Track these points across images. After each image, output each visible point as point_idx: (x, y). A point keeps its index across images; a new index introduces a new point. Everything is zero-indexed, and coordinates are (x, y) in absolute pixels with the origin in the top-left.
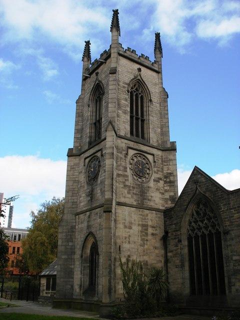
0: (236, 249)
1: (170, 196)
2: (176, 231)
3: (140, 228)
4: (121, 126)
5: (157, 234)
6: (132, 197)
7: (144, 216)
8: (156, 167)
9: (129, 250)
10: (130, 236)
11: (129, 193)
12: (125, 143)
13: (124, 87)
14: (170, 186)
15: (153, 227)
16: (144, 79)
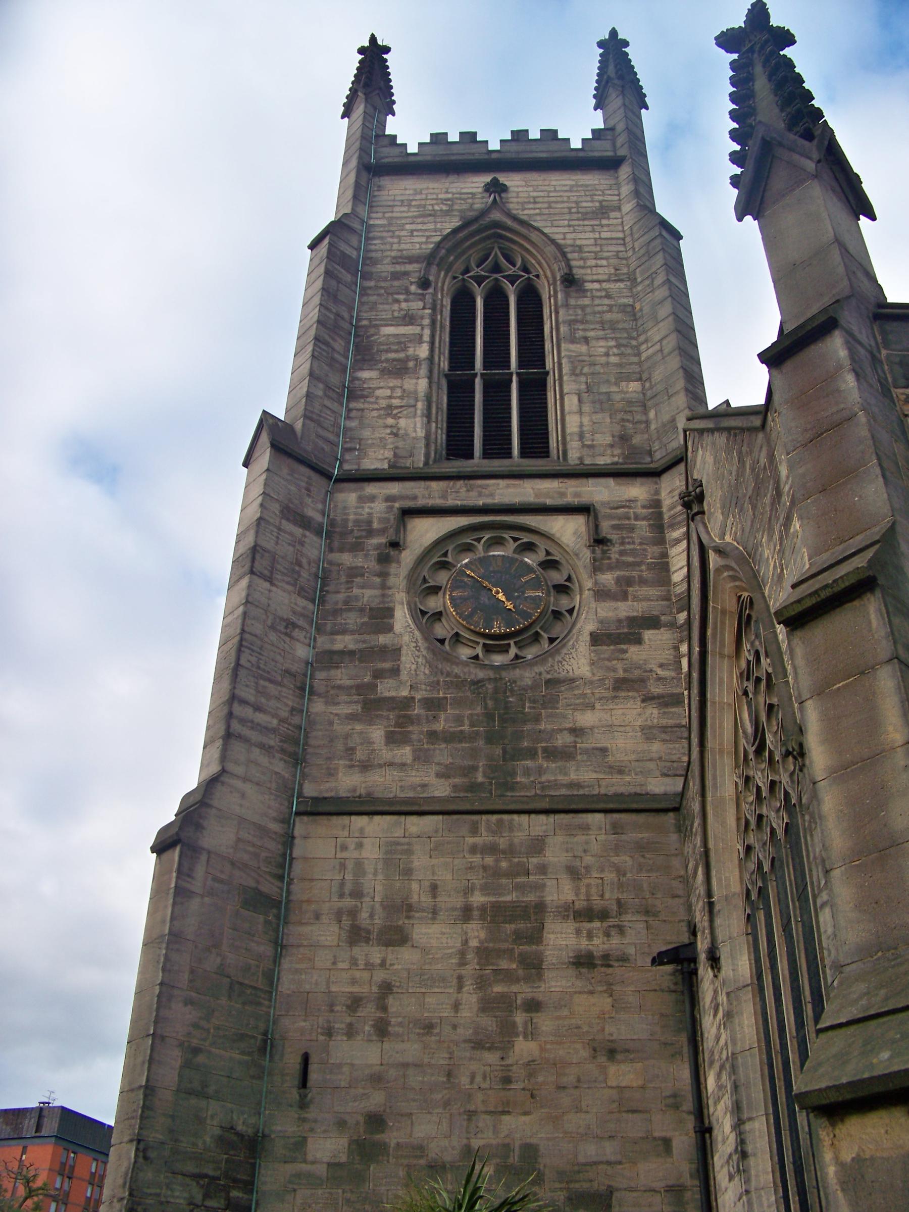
3: (476, 932)
4: (366, 433)
5: (624, 959)
6: (422, 757)
7: (511, 851)
8: (610, 568)
9: (377, 1079)
10: (387, 988)
11: (392, 739)
12: (389, 499)
13: (396, 276)
15: (587, 914)
16: (523, 215)
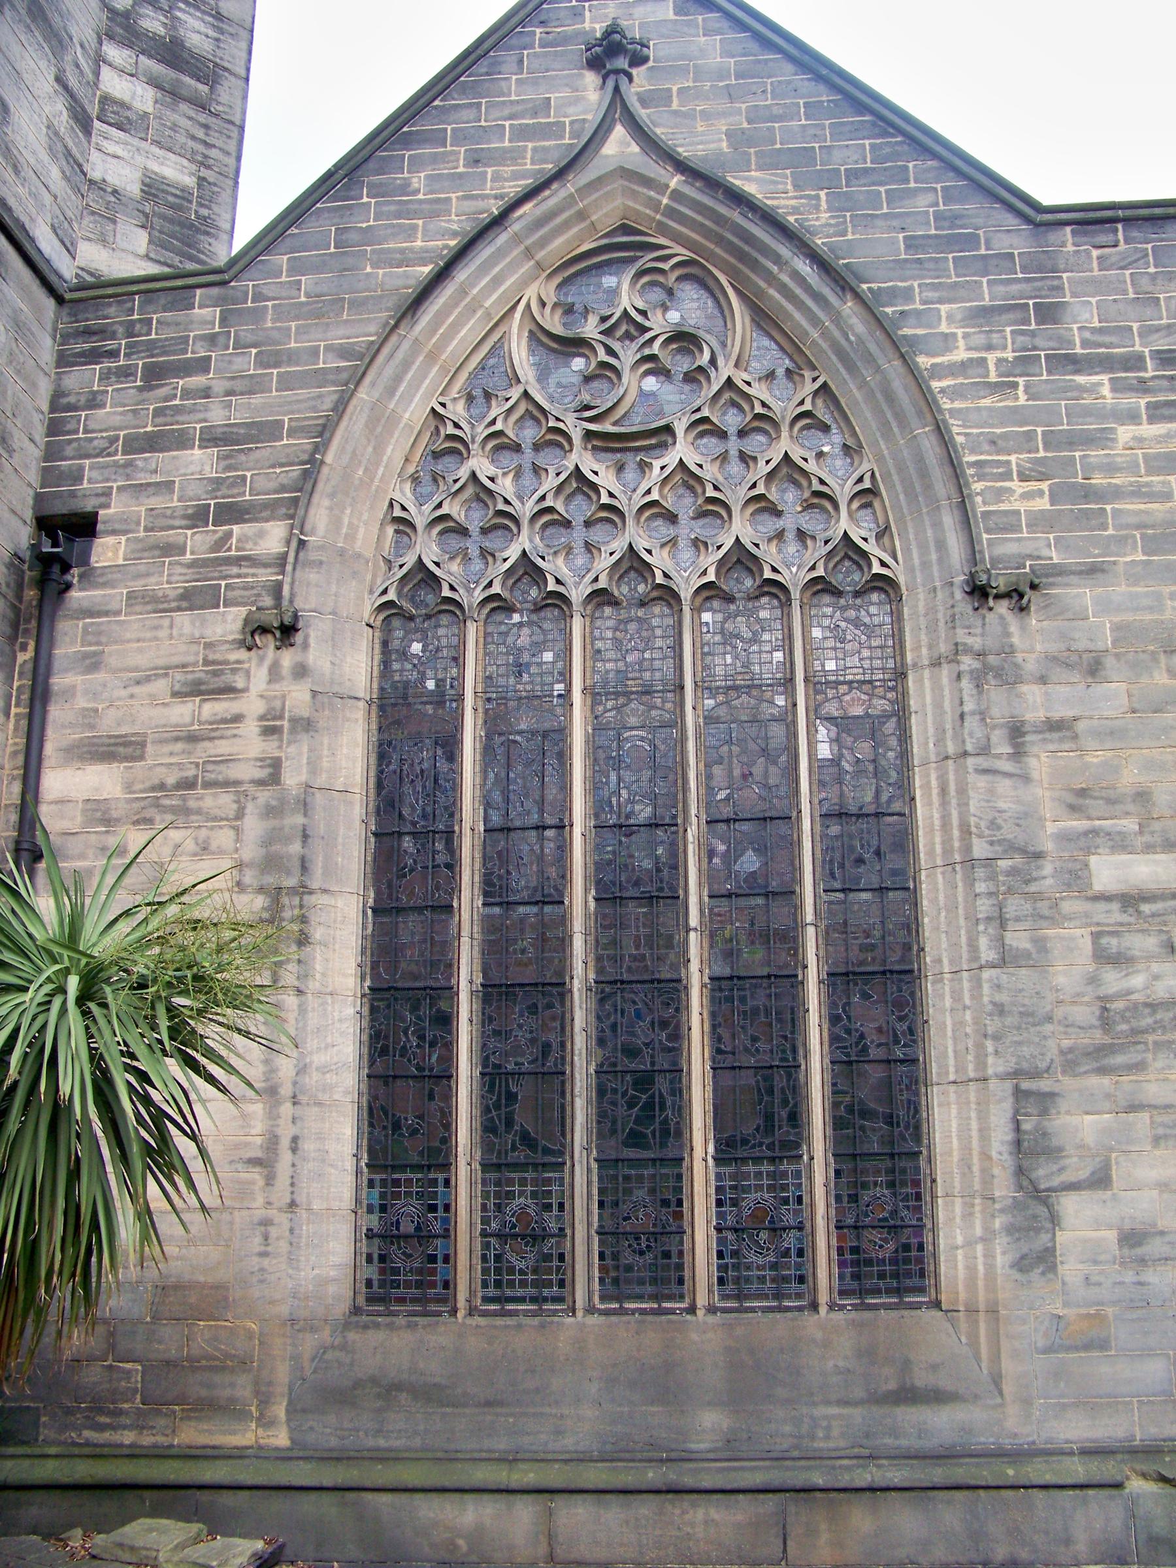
0: (1130, 777)
1: (152, 188)
2: (232, 513)
14: (171, 94)
